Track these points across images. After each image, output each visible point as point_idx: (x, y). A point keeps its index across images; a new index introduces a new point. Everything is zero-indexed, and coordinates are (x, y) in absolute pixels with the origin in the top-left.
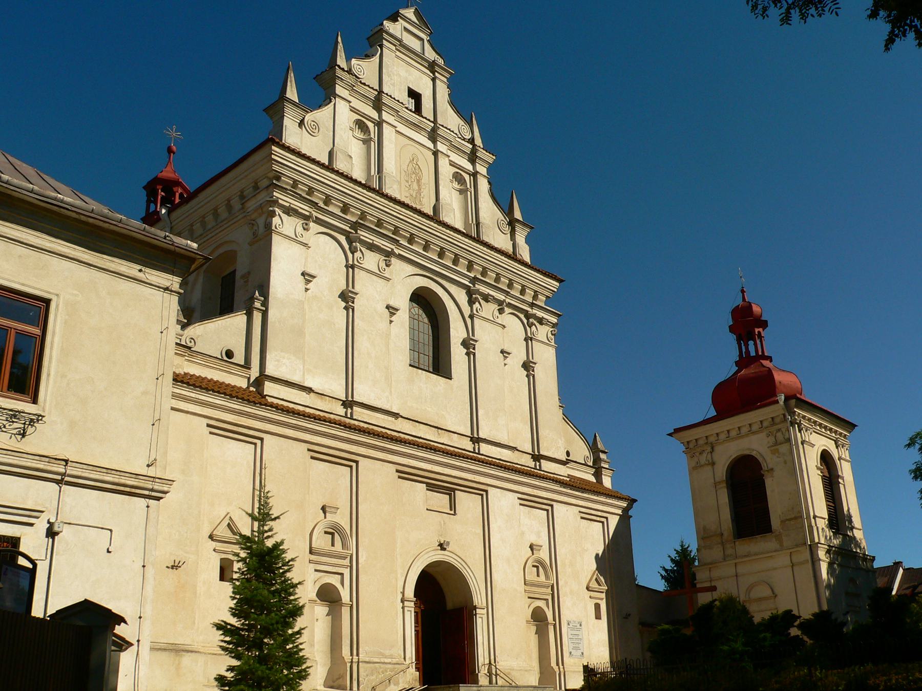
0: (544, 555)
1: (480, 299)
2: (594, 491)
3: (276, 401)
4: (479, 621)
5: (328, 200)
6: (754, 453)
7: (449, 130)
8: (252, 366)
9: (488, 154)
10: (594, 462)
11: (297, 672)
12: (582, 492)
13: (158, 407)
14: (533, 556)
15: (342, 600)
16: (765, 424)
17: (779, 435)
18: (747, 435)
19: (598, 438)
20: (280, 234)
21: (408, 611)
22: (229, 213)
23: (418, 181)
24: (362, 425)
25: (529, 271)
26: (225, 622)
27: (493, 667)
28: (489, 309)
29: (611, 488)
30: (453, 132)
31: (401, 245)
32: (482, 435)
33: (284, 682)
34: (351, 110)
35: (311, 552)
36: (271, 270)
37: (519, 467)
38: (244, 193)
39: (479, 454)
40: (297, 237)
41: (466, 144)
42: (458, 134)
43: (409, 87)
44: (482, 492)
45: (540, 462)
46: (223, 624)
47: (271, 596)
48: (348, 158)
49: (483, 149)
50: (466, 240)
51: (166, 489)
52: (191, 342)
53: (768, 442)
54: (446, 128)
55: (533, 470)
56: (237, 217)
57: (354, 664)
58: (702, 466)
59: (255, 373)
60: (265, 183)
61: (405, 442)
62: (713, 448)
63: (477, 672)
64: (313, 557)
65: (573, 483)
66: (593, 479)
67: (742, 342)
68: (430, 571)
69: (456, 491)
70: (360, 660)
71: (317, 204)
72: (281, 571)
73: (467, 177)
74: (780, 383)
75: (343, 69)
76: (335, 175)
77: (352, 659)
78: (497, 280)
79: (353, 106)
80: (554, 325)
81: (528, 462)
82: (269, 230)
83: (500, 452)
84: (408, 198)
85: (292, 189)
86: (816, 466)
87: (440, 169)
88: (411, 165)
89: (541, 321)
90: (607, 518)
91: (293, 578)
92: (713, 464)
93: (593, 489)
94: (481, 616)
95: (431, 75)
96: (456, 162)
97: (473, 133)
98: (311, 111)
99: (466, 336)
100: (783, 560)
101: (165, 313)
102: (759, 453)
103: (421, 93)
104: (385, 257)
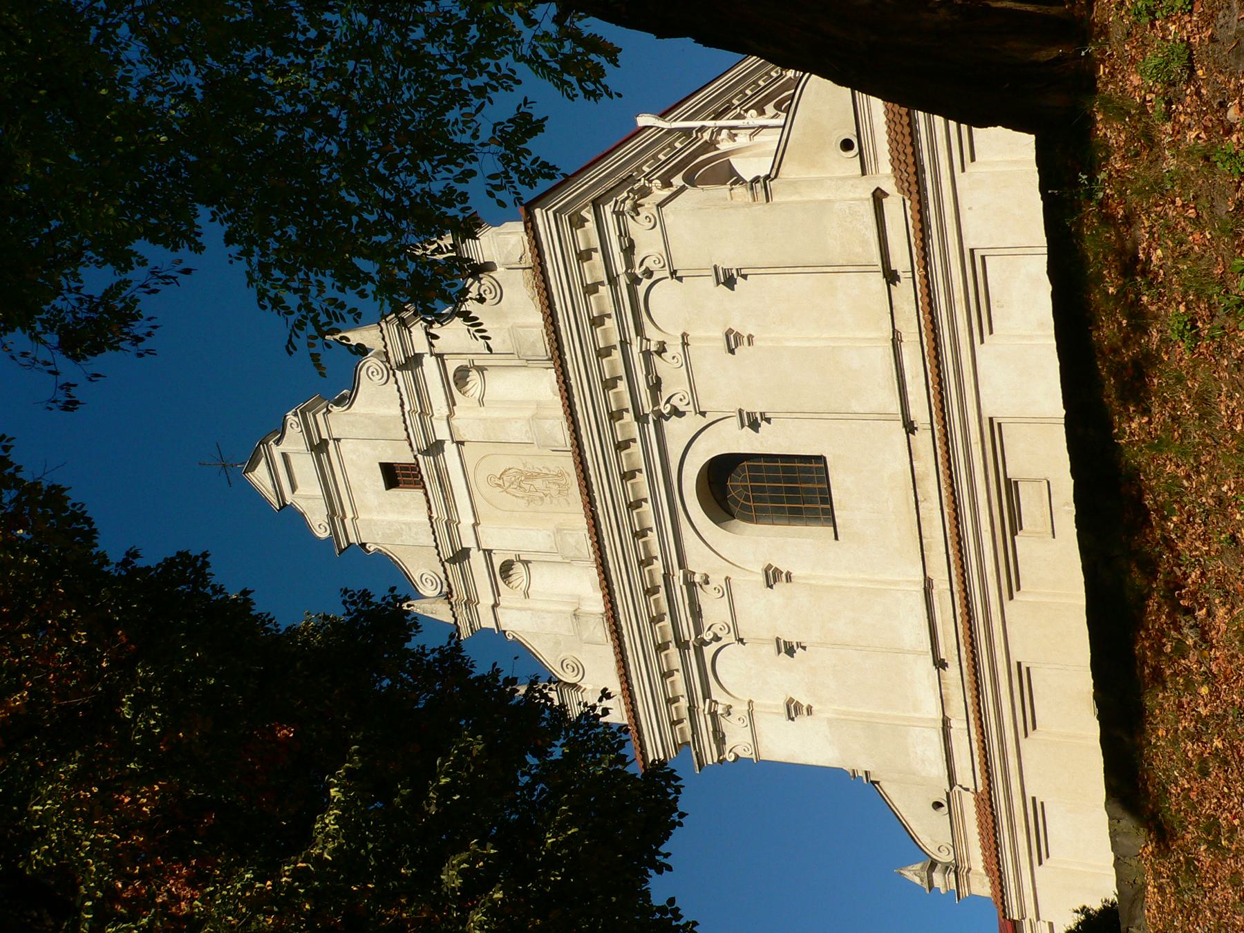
23: (527, 478)
25: (554, 290)
28: (675, 386)
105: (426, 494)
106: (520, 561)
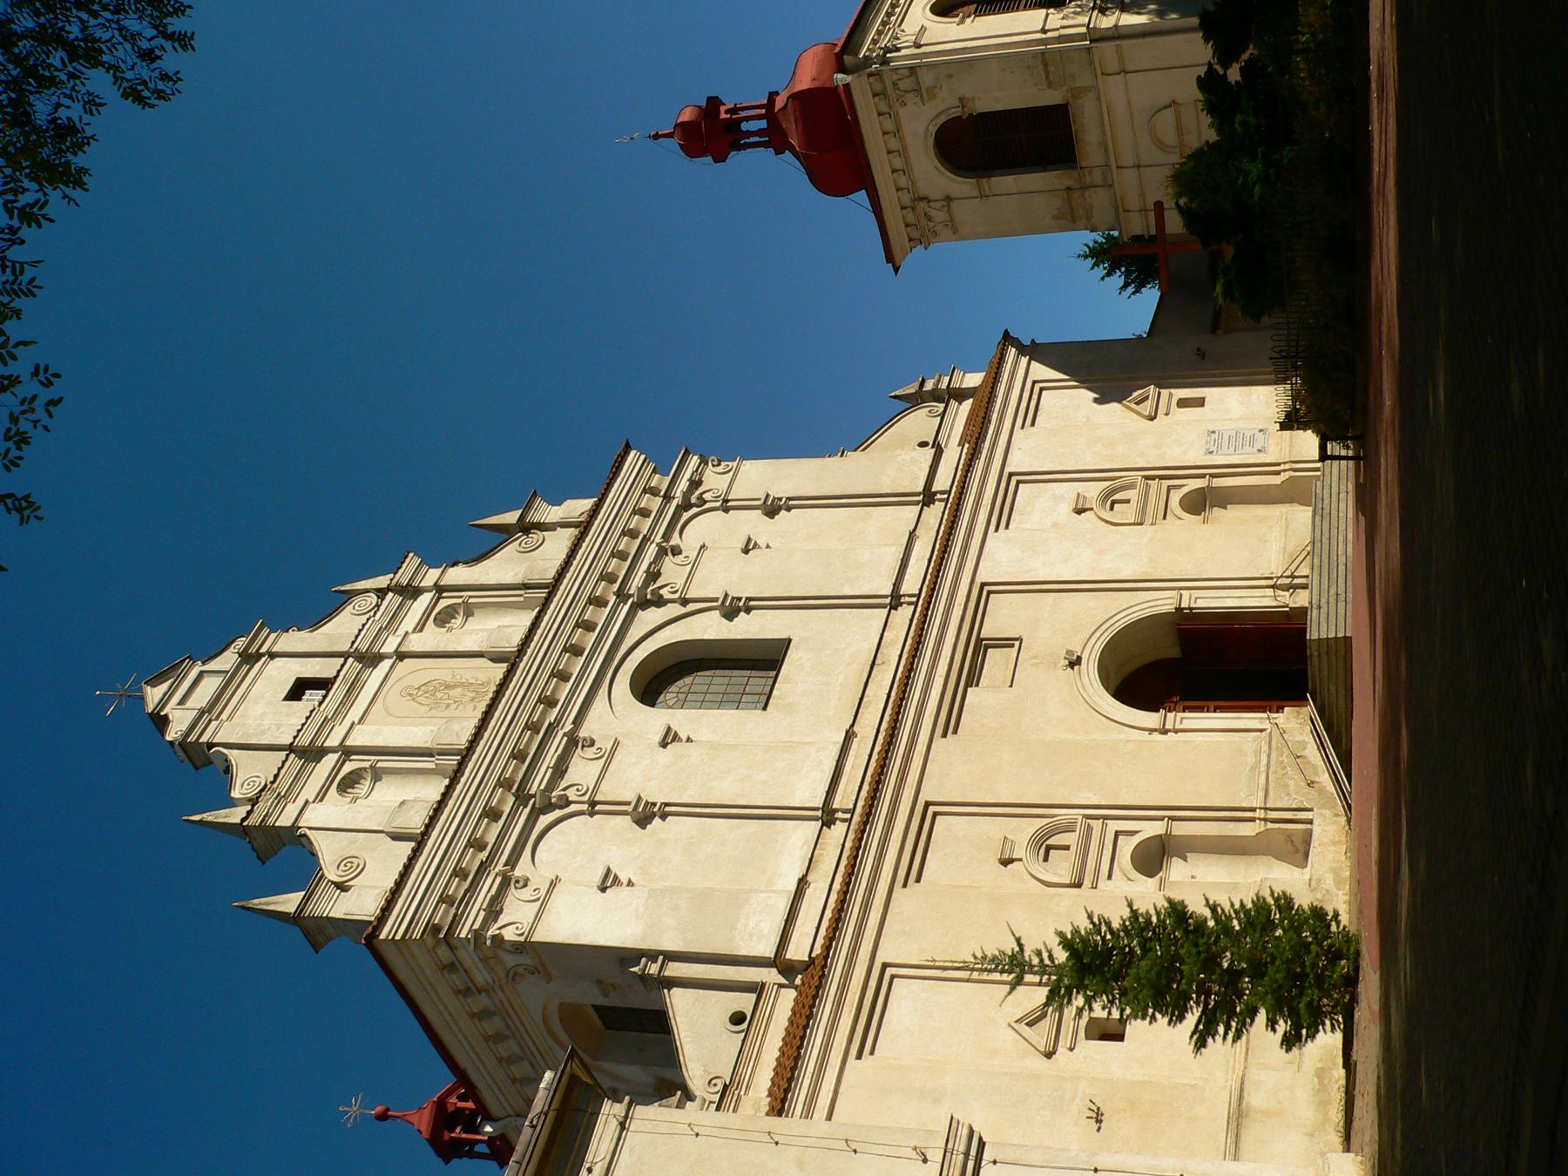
0: (1093, 490)
1: (655, 586)
2: (988, 403)
3: (820, 941)
4: (1201, 603)
5: (476, 844)
6: (933, 129)
7: (360, 631)
8: (759, 980)
9: (404, 566)
10: (939, 400)
11: (1280, 913)
12: (990, 422)
13: (824, 1143)
14: (1095, 509)
15: (1161, 835)
16: (883, 107)
17: (903, 85)
18: (902, 140)
19: (897, 393)
20: (532, 928)
21: (1181, 723)
22: (495, 1014)
23: (448, 687)
24: (864, 794)
26: (1194, 1033)
27: (1279, 582)
28: (672, 572)
29: (984, 373)
30: (364, 625)
31: (558, 720)
32: (888, 590)
33: (1295, 936)
34: (321, 800)
35: (1079, 885)
36: (595, 944)
37: (942, 528)
38: (461, 987)
39: (919, 596)
40: (539, 899)
41: (386, 603)
42: (367, 616)
43: (286, 699)
44: (984, 592)
45: (935, 493)
46: (1195, 1037)
47: (1150, 954)
48: (404, 807)
49: (395, 574)
50: (552, 606)
51: (965, 1131)
52: (715, 1085)
53: (915, 103)
54: (357, 637)
55: (949, 505)
56: (501, 1001)
57: (1269, 816)
58: (952, 220)
59: (771, 976)
60: (443, 952)
61: (896, 721)
62: (922, 199)
63: (1287, 609)
64: (1087, 882)
65: (974, 438)
66: (968, 404)
67: (742, 142)
68: (1113, 685)
69: (981, 636)
70: (1263, 806)
71: (482, 863)
72: (1109, 937)
73: (443, 603)
74: (814, 80)
75: (249, 813)
76: (433, 831)
77: (1260, 819)
78: (622, 556)
79: (314, 796)
80: (704, 461)
81: (935, 513)
82: (525, 947)
83: (917, 560)
84: (478, 705)
85: (456, 905)
86: (958, 25)
87: (428, 648)
88: (419, 699)
89: (695, 484)
90: (1034, 382)
91: (1121, 917)
92: (948, 199)
93: (984, 404)
94: (1193, 599)
95: (263, 659)
96: (416, 620)
97: (367, 591)
98: (321, 869)
99: (718, 612)
100: (1114, 88)
101: (665, 1128)
102: (931, 121)
103: (294, 679)
104: (577, 748)
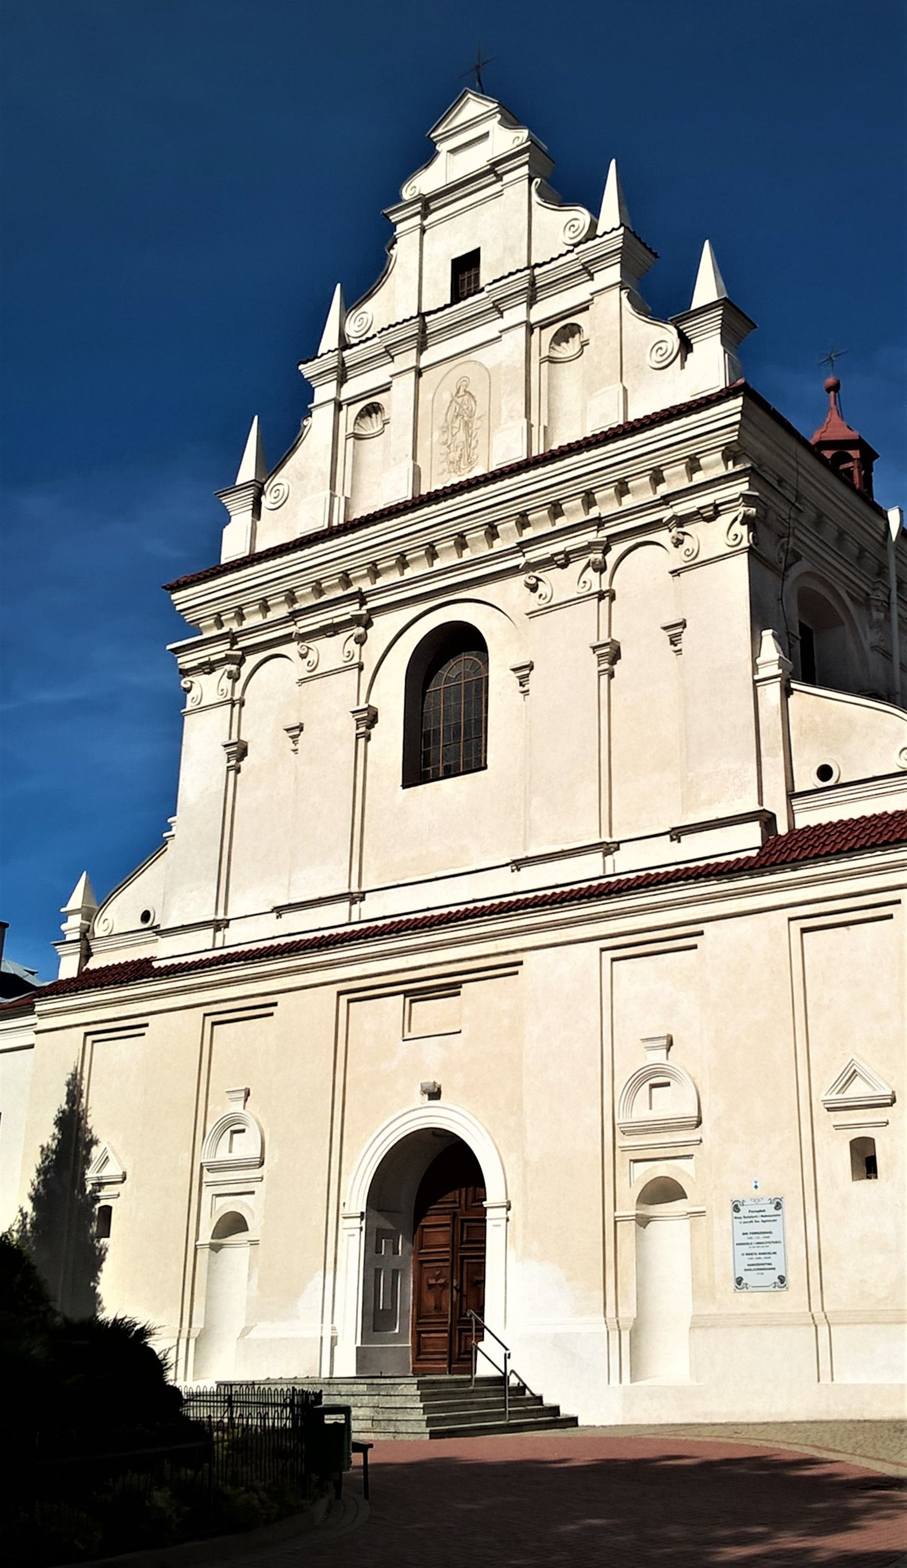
7: (511, 274)
23: (466, 424)
105: (447, 306)
106: (384, 424)
